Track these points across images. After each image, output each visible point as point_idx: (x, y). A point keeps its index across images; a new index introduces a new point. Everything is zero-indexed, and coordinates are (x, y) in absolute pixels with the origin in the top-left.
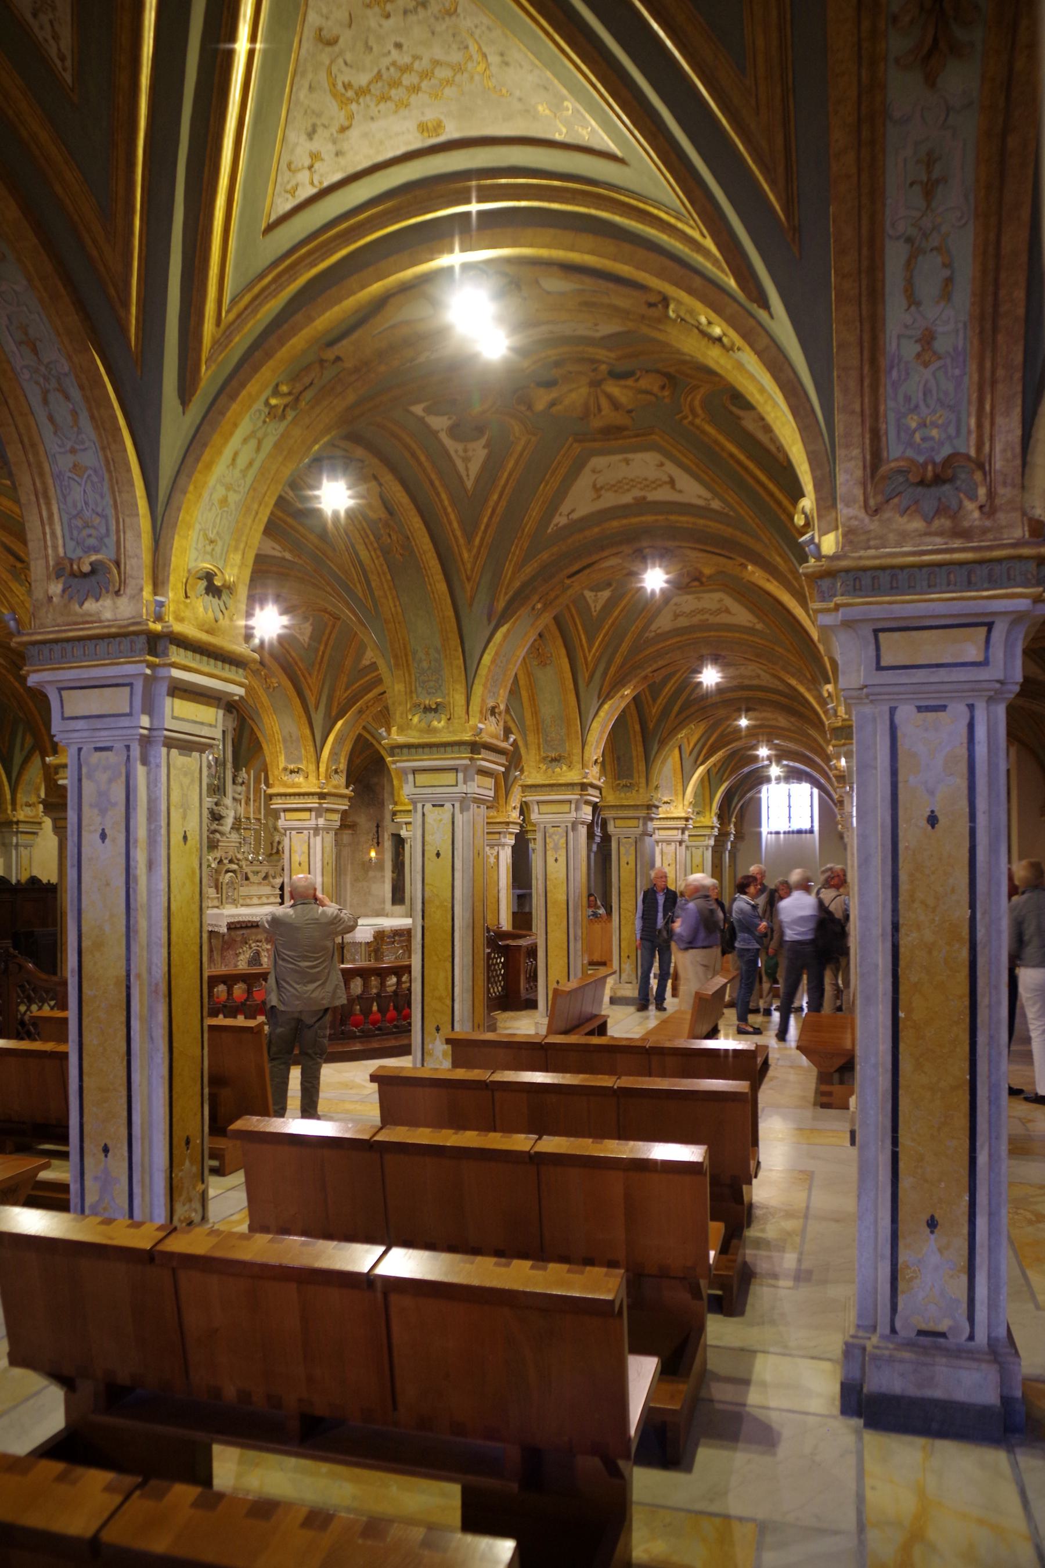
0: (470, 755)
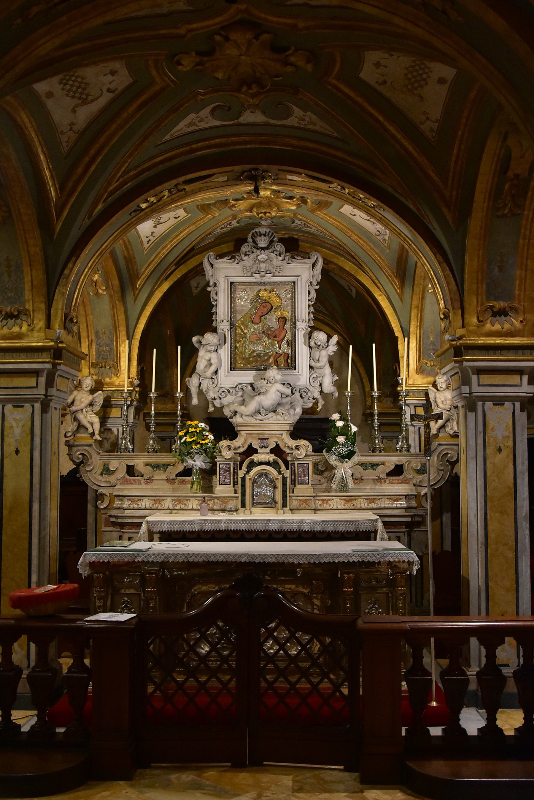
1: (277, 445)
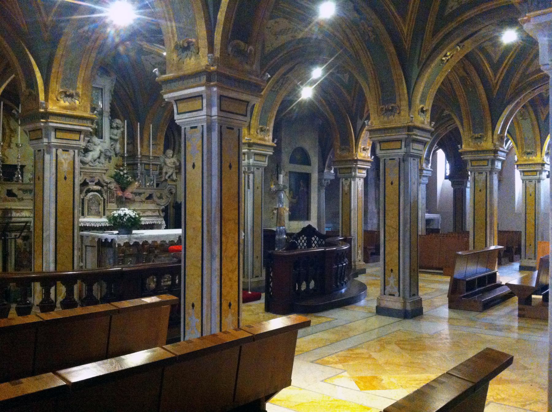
0: (407, 133)
1: (99, 181)
